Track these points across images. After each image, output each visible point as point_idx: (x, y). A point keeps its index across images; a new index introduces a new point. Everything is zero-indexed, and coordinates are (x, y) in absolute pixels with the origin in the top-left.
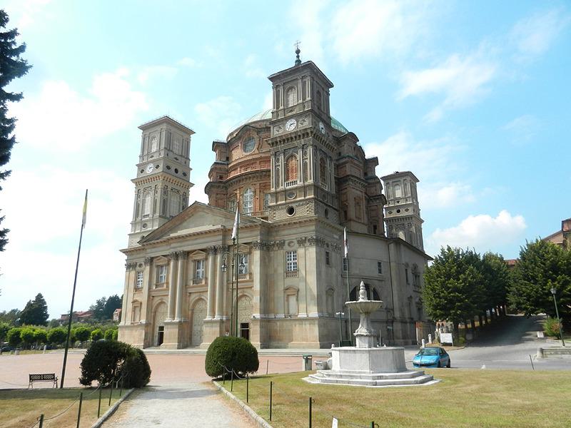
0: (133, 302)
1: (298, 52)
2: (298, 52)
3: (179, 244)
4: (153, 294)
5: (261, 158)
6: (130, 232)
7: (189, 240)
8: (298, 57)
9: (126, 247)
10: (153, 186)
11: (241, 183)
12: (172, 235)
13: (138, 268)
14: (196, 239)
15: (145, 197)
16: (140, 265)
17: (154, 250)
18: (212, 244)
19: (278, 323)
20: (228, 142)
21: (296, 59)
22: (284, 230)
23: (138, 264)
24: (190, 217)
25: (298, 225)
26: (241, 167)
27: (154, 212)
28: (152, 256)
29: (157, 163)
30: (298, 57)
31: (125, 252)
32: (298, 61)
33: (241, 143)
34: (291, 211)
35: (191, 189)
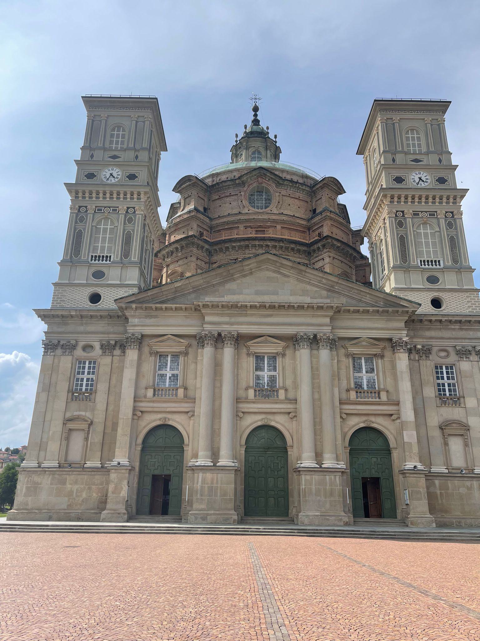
0: (67, 421)
1: (256, 109)
2: (256, 109)
3: (226, 319)
4: (143, 405)
5: (283, 222)
6: (56, 280)
7: (252, 315)
8: (256, 115)
9: (48, 305)
10: (122, 207)
11: (247, 251)
12: (208, 299)
13: (79, 352)
14: (271, 316)
15: (99, 223)
16: (88, 348)
17: (148, 321)
18: (310, 330)
19: (437, 482)
20: (213, 186)
21: (253, 118)
22: (429, 329)
23: (81, 344)
24: (245, 276)
25: (457, 326)
26: (246, 227)
27: (126, 254)
28: (148, 331)
29: (132, 171)
30: (256, 115)
31: (43, 315)
32: (256, 122)
33: (245, 192)
34: (436, 303)
35: (465, 204)
